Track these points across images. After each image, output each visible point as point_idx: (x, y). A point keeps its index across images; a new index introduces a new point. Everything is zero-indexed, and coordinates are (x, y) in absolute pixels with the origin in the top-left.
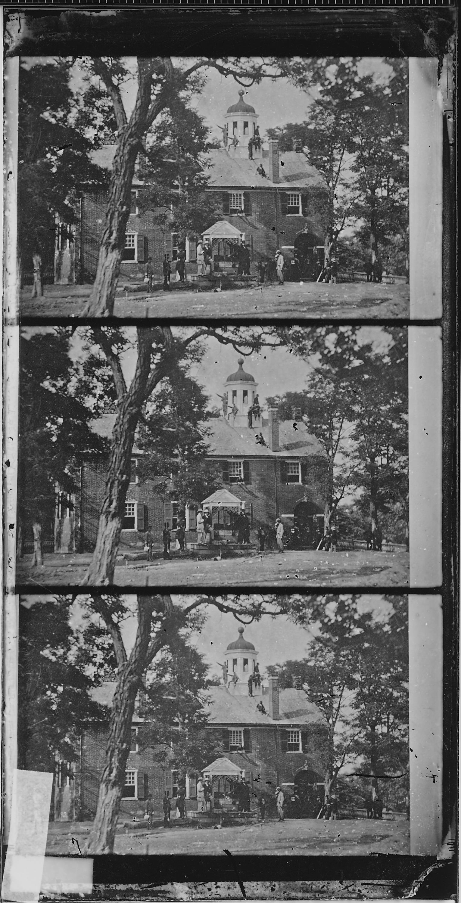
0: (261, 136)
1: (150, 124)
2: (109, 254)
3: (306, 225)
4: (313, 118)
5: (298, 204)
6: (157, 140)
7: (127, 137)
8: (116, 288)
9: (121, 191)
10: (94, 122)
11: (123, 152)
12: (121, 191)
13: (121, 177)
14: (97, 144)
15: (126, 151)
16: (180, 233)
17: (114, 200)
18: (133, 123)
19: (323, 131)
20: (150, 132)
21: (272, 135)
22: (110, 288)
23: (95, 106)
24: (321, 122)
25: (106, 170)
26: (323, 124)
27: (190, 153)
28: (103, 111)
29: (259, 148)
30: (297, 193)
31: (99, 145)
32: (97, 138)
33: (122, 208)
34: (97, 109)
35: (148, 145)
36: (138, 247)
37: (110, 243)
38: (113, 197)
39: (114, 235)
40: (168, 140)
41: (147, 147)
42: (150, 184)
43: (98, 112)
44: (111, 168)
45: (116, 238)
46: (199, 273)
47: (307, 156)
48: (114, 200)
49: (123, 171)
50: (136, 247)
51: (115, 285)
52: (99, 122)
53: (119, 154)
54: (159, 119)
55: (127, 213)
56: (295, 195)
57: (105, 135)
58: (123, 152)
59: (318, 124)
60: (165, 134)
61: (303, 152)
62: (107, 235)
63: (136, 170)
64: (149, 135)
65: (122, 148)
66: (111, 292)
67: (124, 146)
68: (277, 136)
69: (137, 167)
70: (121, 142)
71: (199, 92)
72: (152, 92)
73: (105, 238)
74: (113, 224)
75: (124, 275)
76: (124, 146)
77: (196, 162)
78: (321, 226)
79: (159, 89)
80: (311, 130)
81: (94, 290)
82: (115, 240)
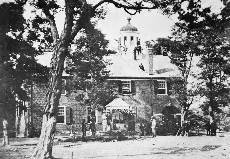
0: (141, 45)
1: (73, 39)
2: (49, 119)
3: (170, 101)
4: (173, 34)
5: (165, 87)
6: (78, 48)
7: (59, 46)
8: (53, 140)
9: (56, 80)
10: (39, 38)
11: (56, 56)
12: (56, 80)
13: (55, 72)
14: (40, 52)
15: (58, 56)
16: (92, 106)
17: (51, 86)
18: (63, 38)
19: (180, 42)
20: (73, 43)
21: (148, 45)
22: (50, 140)
23: (39, 27)
24: (179, 37)
25: (46, 67)
26: (180, 38)
27: (98, 57)
28: (44, 31)
29: (141, 53)
30: (164, 81)
31: (42, 52)
32: (40, 48)
33: (56, 91)
34: (41, 29)
35: (72, 52)
36: (66, 115)
37: (50, 112)
38: (51, 84)
39: (52, 107)
40: (84, 49)
41: (71, 53)
42: (73, 75)
43: (41, 31)
44: (49, 66)
45: (53, 109)
46: (104, 131)
47: (170, 57)
48: (51, 86)
49: (57, 68)
50: (65, 115)
51: (52, 138)
52: (41, 38)
53: (54, 57)
54: (79, 35)
55: (60, 94)
56: (163, 82)
57: (46, 45)
58: (56, 56)
59: (177, 38)
60: (82, 45)
61: (167, 55)
62: (47, 108)
63: (65, 67)
64: (72, 45)
65: (56, 53)
66: (50, 142)
67: (57, 52)
68: (152, 45)
69: (65, 65)
70: (55, 50)
71: (103, 18)
72: (74, 19)
73: (46, 110)
74: (51, 101)
75: (58, 132)
76: (57, 52)
77: (101, 62)
78: (179, 101)
79: (79, 17)
80: (173, 41)
81: (40, 141)
82: (52, 110)
